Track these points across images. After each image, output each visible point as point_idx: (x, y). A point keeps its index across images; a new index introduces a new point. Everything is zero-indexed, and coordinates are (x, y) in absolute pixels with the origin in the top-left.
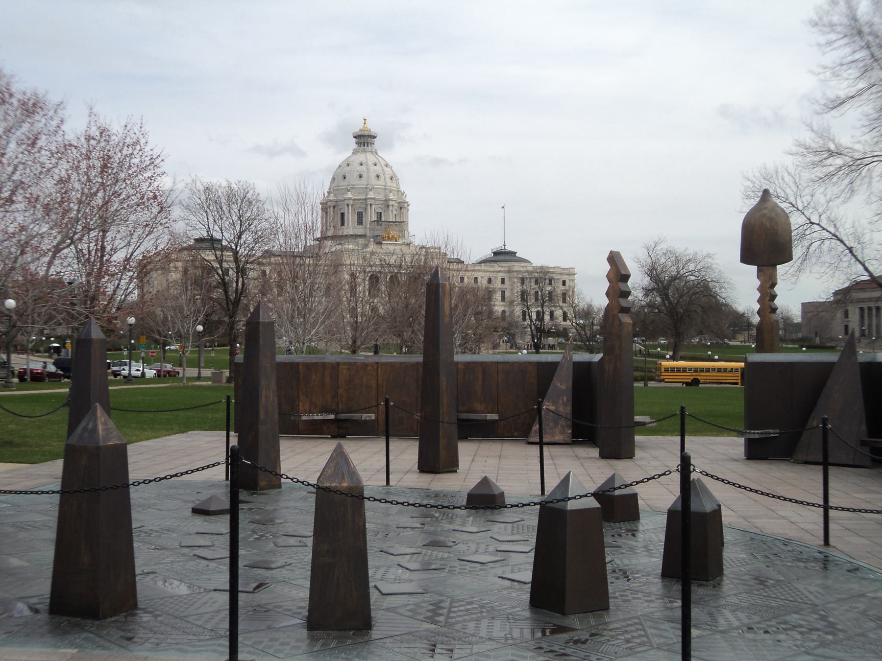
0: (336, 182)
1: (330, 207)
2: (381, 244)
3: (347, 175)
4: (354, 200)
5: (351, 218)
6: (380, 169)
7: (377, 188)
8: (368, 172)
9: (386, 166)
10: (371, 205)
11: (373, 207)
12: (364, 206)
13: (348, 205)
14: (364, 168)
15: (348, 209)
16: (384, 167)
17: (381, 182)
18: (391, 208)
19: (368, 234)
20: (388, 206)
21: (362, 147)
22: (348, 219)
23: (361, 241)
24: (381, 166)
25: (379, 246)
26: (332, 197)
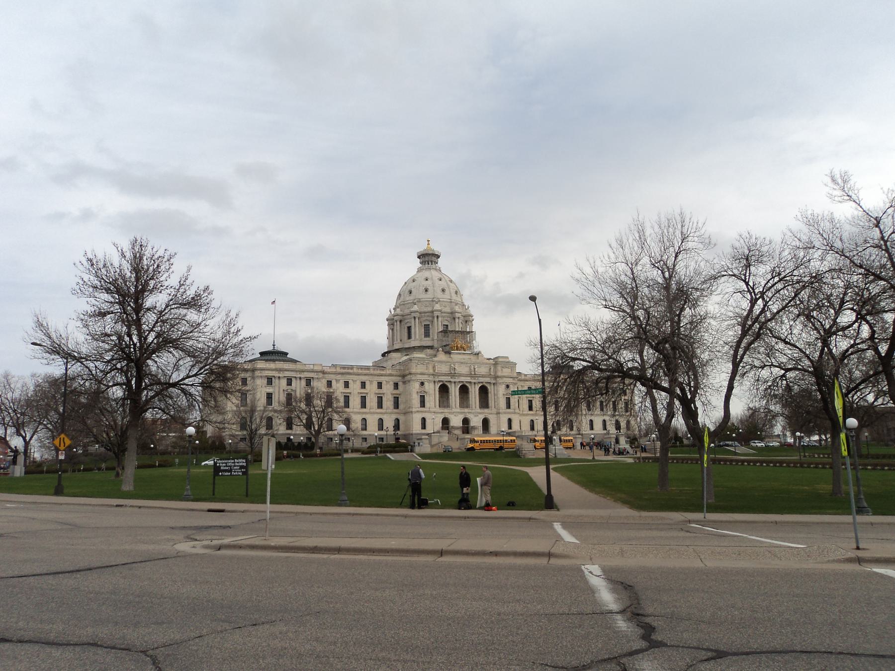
0: (402, 297)
1: (396, 321)
2: (450, 353)
3: (413, 290)
4: (420, 313)
5: (417, 331)
6: (445, 284)
7: (443, 301)
8: (433, 287)
9: (451, 281)
10: (438, 317)
11: (440, 319)
12: (431, 318)
13: (415, 318)
14: (429, 282)
15: (415, 322)
16: (449, 283)
17: (446, 296)
18: (457, 320)
19: (436, 346)
20: (454, 319)
21: (427, 265)
22: (415, 332)
23: (429, 351)
24: (446, 281)
25: (448, 355)
26: (398, 311)
